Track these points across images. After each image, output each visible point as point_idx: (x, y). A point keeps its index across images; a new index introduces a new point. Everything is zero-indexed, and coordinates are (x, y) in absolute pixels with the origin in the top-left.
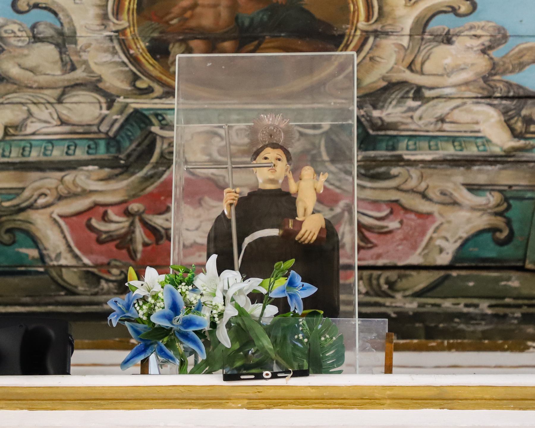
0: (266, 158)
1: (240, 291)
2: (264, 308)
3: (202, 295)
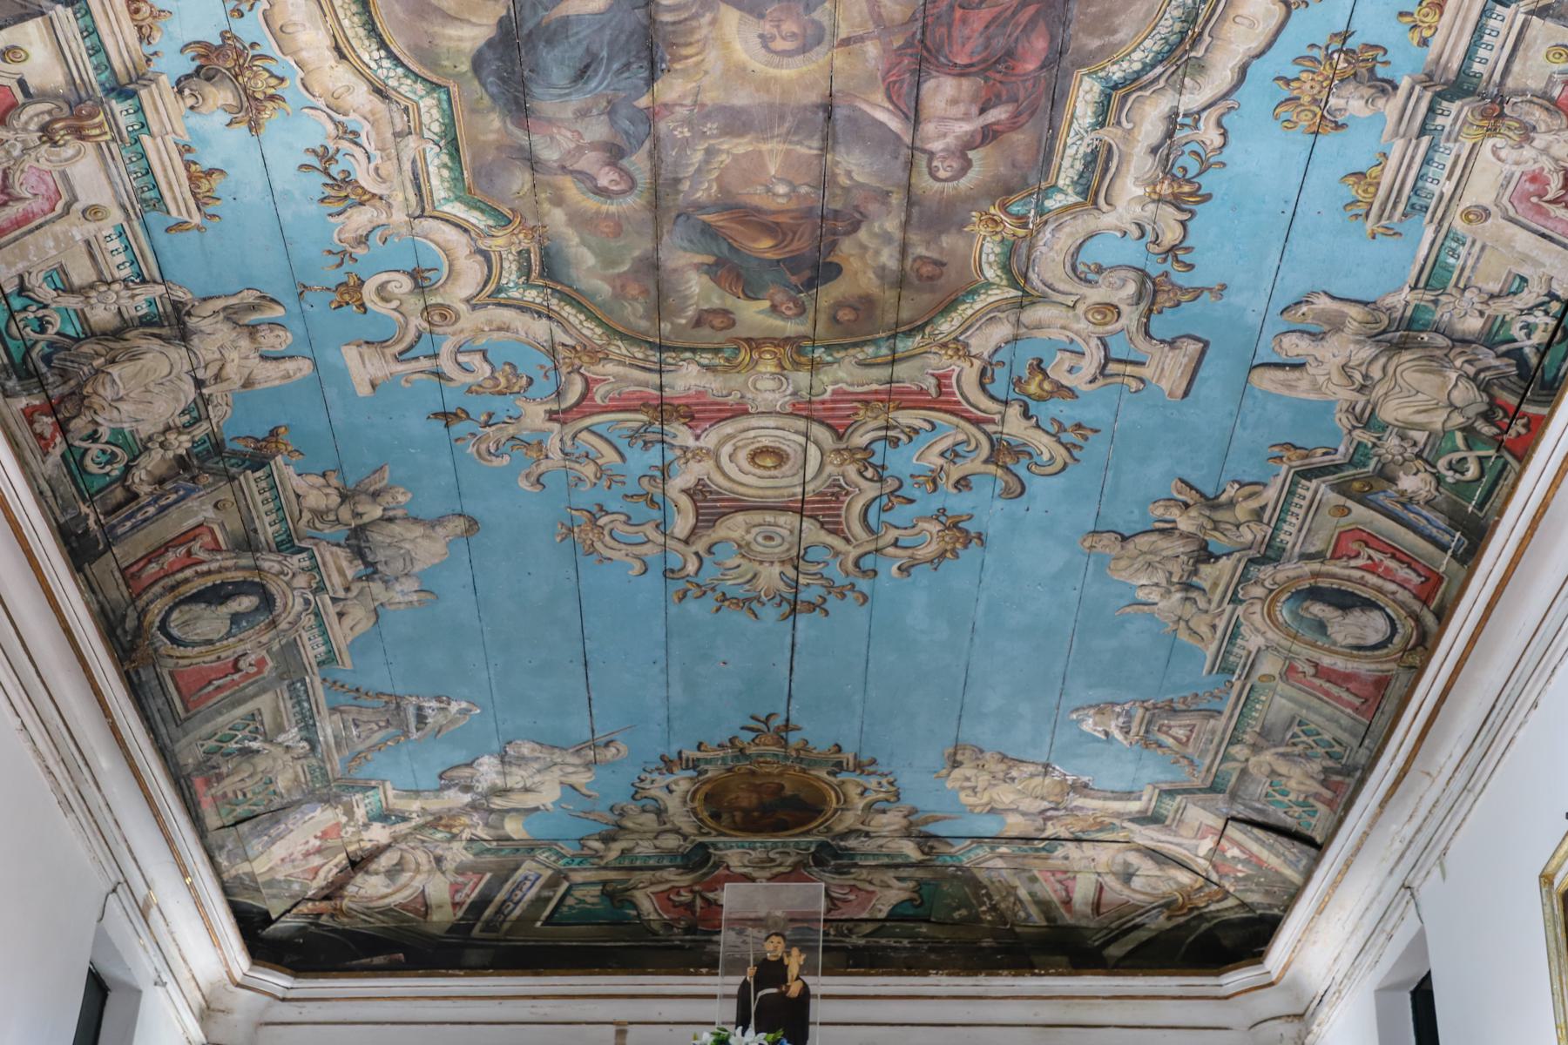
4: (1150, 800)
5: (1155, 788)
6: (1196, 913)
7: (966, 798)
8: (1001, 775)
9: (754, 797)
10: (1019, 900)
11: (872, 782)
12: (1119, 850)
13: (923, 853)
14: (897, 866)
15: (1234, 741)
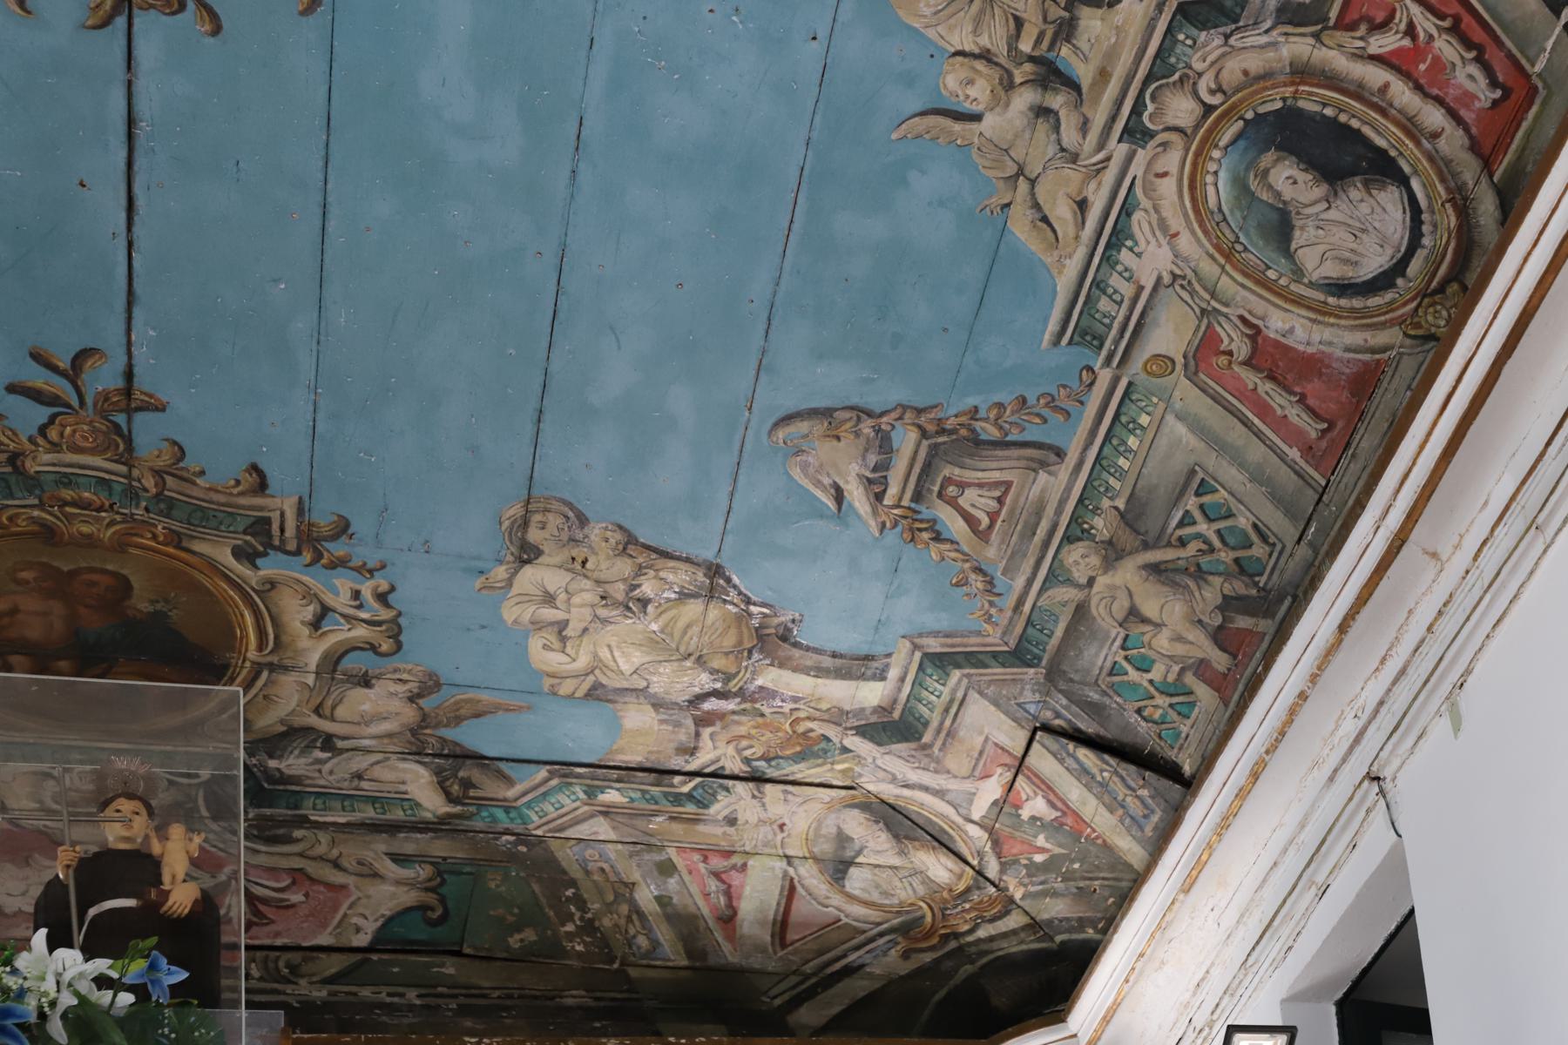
0: (118, 811)
1: (81, 975)
2: (115, 996)
3: (25, 978)
4: (902, 680)
5: (916, 647)
6: (953, 944)
7: (543, 656)
8: (618, 591)
9: (57, 608)
10: (637, 911)
11: (339, 590)
12: (831, 806)
13: (451, 799)
14: (393, 828)
15: (1076, 532)
